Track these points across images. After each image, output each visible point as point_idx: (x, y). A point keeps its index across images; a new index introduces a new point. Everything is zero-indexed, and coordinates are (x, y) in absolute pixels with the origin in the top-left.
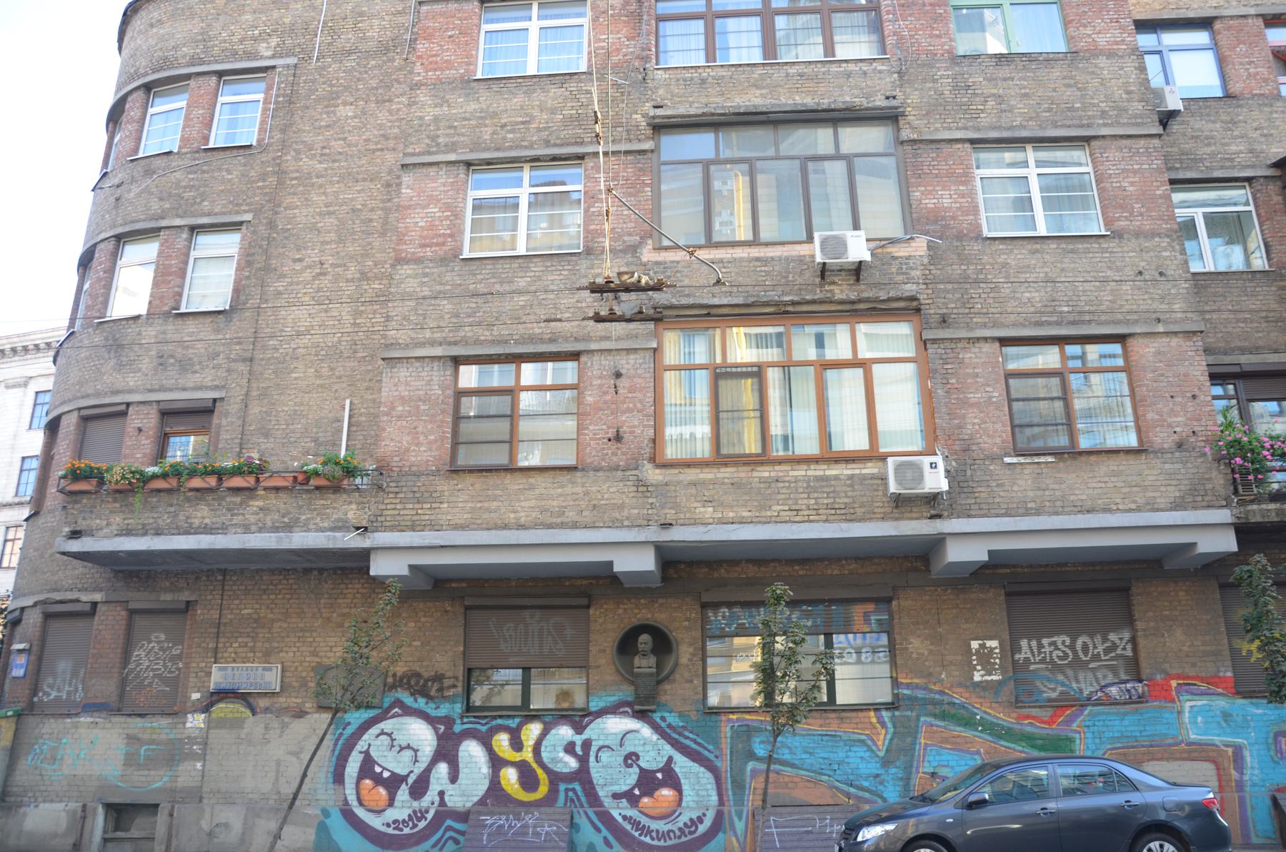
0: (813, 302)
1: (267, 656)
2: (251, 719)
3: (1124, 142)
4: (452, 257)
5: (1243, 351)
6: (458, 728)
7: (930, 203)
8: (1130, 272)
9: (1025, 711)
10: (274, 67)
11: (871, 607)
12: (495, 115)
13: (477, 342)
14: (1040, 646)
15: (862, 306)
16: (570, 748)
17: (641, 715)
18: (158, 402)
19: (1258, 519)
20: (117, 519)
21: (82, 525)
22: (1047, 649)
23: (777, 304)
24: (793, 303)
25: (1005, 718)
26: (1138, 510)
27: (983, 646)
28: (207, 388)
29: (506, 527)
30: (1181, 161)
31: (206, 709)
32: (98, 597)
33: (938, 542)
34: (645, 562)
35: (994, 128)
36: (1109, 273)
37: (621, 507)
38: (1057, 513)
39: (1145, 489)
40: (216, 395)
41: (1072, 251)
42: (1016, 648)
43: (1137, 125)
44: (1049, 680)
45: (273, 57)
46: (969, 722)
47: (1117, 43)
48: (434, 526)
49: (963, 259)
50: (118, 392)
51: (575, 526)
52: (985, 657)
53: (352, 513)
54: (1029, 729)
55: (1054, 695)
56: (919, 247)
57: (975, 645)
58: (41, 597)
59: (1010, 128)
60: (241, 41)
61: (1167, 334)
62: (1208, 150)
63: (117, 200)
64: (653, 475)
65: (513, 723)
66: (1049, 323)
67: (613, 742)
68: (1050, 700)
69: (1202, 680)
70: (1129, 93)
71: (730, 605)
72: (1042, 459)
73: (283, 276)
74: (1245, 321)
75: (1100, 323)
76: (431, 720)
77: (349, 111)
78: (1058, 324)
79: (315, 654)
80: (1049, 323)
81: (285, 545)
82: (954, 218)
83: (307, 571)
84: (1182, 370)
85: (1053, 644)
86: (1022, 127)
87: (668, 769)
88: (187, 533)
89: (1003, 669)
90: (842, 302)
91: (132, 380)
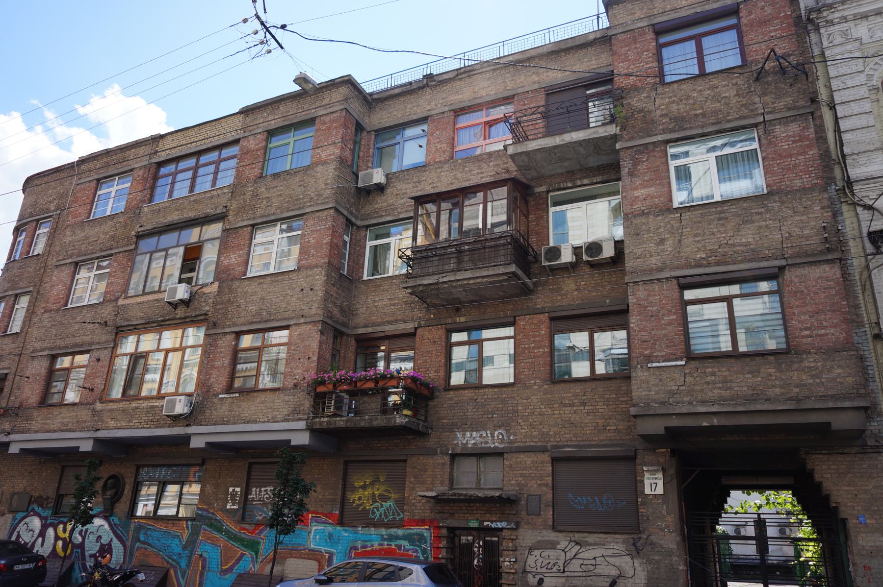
0: (169, 320)
3: (318, 214)
5: (389, 323)
6: (48, 522)
7: (226, 262)
8: (298, 290)
9: (244, 526)
11: (197, 468)
14: (260, 492)
15: (188, 320)
16: (80, 533)
17: (106, 518)
19: (318, 427)
22: (263, 494)
23: (157, 322)
24: (163, 321)
25: (234, 528)
26: (268, 421)
27: (234, 490)
30: (386, 211)
33: (187, 439)
35: (262, 217)
36: (289, 292)
37: (86, 421)
38: (234, 424)
39: (274, 411)
40: (6, 371)
41: (276, 281)
42: (247, 492)
43: (323, 203)
44: (260, 510)
46: (219, 530)
47: (330, 155)
48: (28, 431)
49: (231, 291)
51: (70, 430)
52: (234, 494)
54: (243, 535)
55: (260, 518)
56: (215, 287)
57: (231, 489)
59: (269, 215)
61: (305, 323)
62: (401, 201)
66: (256, 322)
67: (94, 530)
68: (258, 521)
69: (324, 515)
70: (326, 184)
71: (148, 466)
72: (234, 395)
74: (394, 305)
75: (277, 320)
76: (41, 518)
78: (259, 322)
80: (256, 322)
82: (233, 269)
84: (307, 343)
85: (266, 491)
86: (274, 214)
87: (110, 544)
89: (239, 503)
90: (180, 319)
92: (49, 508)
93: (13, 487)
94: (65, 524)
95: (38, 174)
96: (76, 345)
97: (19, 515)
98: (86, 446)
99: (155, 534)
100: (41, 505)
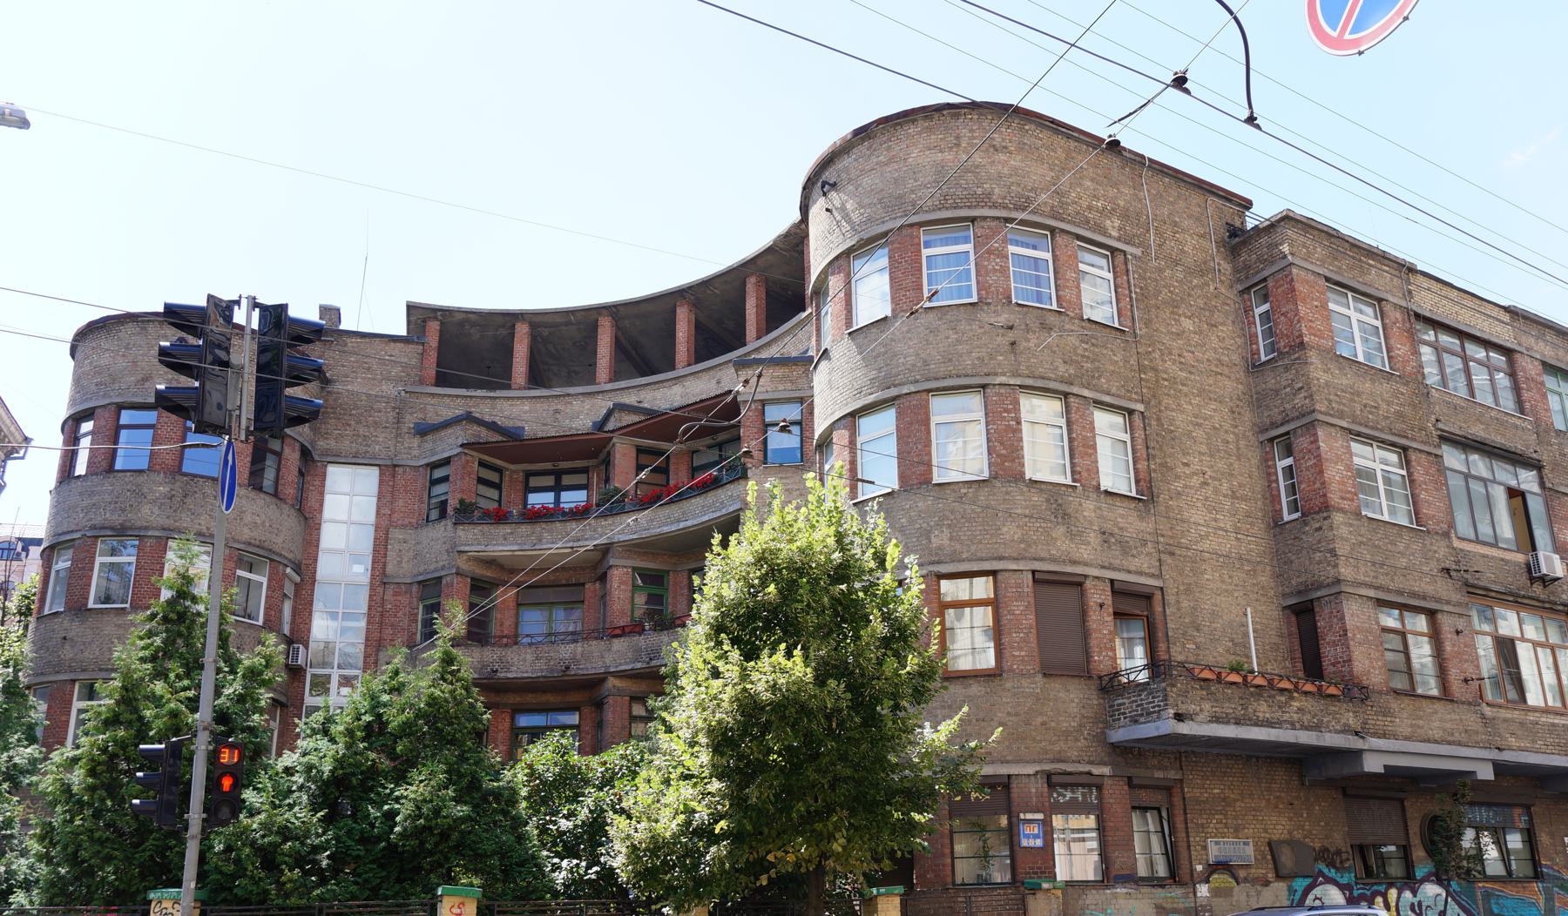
1: (1237, 831)
2: (1237, 888)
4: (1358, 514)
6: (1356, 893)
10: (1125, 252)
12: (1359, 394)
13: (1389, 591)
17: (1439, 882)
18: (1112, 581)
20: (1207, 706)
21: (1183, 709)
29: (1428, 741)
31: (1207, 881)
32: (1106, 770)
34: (1486, 773)
45: (1119, 239)
50: (1074, 563)
51: (1460, 744)
53: (1351, 719)
58: (1048, 767)
60: (1090, 208)
63: (1013, 344)
64: (1488, 711)
65: (1382, 888)
73: (1178, 477)
76: (1341, 887)
77: (1188, 324)
79: (1266, 831)
81: (1321, 743)
83: (1249, 758)
88: (1256, 725)
91: (1085, 553)
92: (1348, 870)
94: (1385, 896)
97: (1301, 884)
98: (1486, 773)
99: (1508, 903)
100: (1331, 864)
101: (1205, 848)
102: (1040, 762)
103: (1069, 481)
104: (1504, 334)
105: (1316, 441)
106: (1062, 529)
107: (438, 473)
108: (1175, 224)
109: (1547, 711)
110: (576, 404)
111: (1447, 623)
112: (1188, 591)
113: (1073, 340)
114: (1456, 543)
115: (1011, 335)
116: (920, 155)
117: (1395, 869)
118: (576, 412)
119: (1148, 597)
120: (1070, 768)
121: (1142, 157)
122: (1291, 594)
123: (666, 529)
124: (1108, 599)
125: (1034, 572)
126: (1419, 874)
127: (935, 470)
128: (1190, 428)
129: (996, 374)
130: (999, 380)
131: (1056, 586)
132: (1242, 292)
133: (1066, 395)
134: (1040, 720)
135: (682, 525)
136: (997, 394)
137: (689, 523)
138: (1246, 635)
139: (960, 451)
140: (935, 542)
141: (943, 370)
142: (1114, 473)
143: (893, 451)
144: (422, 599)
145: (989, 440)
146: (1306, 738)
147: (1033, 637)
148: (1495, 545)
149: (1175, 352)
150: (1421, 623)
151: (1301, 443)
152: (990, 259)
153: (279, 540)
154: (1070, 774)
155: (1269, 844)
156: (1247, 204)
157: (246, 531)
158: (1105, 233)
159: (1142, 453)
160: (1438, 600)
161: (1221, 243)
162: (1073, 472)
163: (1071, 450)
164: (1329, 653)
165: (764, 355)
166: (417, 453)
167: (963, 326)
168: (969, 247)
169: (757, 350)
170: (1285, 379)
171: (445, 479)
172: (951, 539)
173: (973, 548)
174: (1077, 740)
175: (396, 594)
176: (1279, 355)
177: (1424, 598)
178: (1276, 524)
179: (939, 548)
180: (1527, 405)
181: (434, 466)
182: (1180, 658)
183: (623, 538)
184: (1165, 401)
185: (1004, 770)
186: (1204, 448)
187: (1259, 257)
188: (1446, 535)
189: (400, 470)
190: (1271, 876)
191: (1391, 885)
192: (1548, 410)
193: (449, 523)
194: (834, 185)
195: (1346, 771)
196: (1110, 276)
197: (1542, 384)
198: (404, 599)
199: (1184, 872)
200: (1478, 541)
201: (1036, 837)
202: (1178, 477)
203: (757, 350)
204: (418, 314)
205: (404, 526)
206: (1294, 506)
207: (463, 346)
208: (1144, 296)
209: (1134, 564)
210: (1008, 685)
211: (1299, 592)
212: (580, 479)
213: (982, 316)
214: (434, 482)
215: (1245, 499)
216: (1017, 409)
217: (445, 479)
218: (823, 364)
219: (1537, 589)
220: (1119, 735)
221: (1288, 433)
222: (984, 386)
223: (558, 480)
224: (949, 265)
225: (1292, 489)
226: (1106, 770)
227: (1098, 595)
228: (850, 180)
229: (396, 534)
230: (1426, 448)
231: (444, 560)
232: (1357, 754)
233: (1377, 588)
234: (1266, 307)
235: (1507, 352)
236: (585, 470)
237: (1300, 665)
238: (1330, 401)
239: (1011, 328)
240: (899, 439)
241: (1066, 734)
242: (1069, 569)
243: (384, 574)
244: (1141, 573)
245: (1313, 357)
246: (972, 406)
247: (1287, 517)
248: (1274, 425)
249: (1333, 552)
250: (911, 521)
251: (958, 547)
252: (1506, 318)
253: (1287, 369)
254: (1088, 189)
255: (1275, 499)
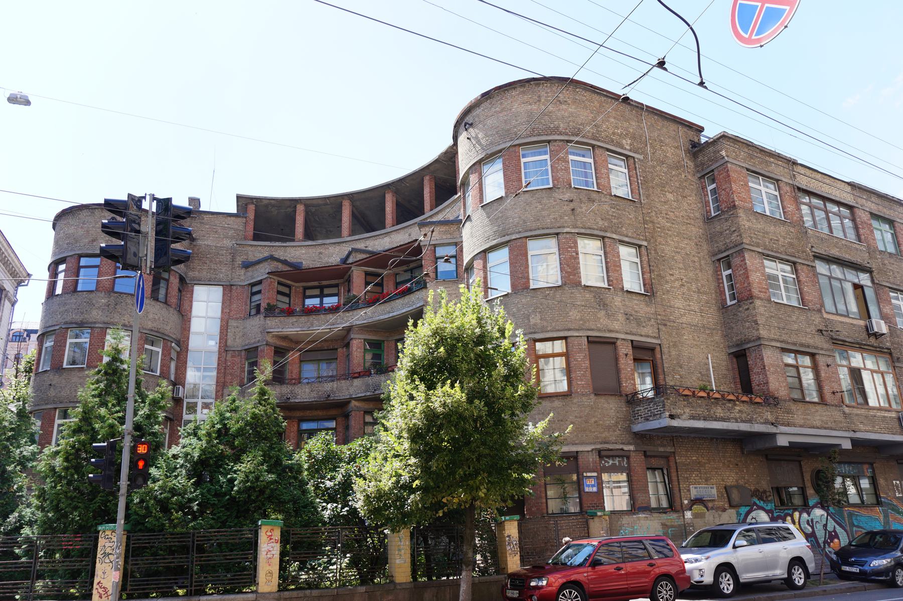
2: (707, 513)
4: (769, 300)
6: (775, 515)
10: (634, 158)
12: (767, 233)
13: (788, 343)
17: (823, 508)
18: (632, 341)
20: (687, 410)
21: (674, 412)
28: (651, 337)
31: (691, 509)
32: (632, 448)
34: (847, 445)
37: (841, 422)
45: (630, 151)
50: (610, 331)
51: (831, 429)
58: (599, 446)
60: (614, 134)
63: (573, 210)
64: (847, 410)
65: (790, 512)
73: (667, 282)
76: (767, 512)
77: (670, 196)
79: (723, 480)
83: (712, 439)
87: (835, 531)
88: (715, 420)
91: (616, 326)
92: (770, 501)
93: (723, 480)
95: (592, 86)
96: (802, 345)
97: (743, 510)
98: (847, 445)
99: (862, 519)
100: (760, 499)
101: (689, 491)
102: (594, 443)
103: (606, 286)
104: (849, 199)
105: (744, 260)
106: (603, 312)
107: (255, 289)
108: (661, 141)
109: (880, 409)
110: (331, 249)
111: (821, 361)
112: (675, 345)
113: (606, 207)
114: (825, 316)
115: (572, 205)
116: (519, 106)
117: (797, 501)
118: (329, 253)
119: (652, 350)
120: (611, 447)
121: (642, 104)
122: (733, 346)
123: (382, 317)
124: (630, 352)
125: (588, 337)
126: (811, 503)
127: (531, 281)
128: (673, 254)
129: (564, 227)
130: (566, 230)
131: (601, 345)
132: (700, 178)
133: (603, 238)
134: (593, 420)
135: (391, 315)
136: (565, 238)
137: (395, 314)
138: (708, 370)
139: (545, 269)
140: (532, 321)
141: (534, 225)
142: (631, 280)
143: (508, 271)
144: (247, 359)
145: (561, 264)
146: (744, 427)
147: (588, 374)
148: (847, 316)
149: (664, 212)
150: (807, 361)
151: (736, 261)
152: (559, 162)
153: (168, 328)
154: (612, 450)
155: (725, 488)
156: (700, 129)
157: (150, 323)
158: (622, 147)
159: (647, 269)
160: (816, 348)
161: (687, 151)
162: (608, 281)
163: (607, 268)
164: (755, 379)
165: (435, 219)
166: (244, 278)
167: (545, 201)
168: (547, 157)
169: (431, 217)
170: (725, 225)
171: (259, 292)
172: (541, 319)
173: (554, 324)
174: (615, 431)
175: (233, 356)
176: (722, 212)
177: (808, 347)
178: (723, 307)
179: (534, 325)
180: (863, 237)
181: (253, 285)
182: (672, 383)
183: (358, 323)
184: (659, 239)
185: (574, 449)
186: (681, 266)
187: (708, 159)
188: (819, 311)
189: (234, 288)
190: (727, 506)
191: (795, 510)
192: (874, 239)
193: (262, 316)
194: (471, 125)
195: (767, 445)
196: (626, 171)
197: (871, 225)
198: (237, 359)
199: (677, 504)
200: (837, 314)
201: (593, 486)
202: (667, 282)
203: (431, 217)
204: (243, 201)
205: (237, 319)
206: (733, 297)
207: (268, 218)
208: (645, 181)
209: (644, 331)
210: (575, 401)
211: (738, 345)
212: (334, 290)
213: (556, 195)
214: (253, 294)
215: (705, 293)
216: (576, 246)
217: (259, 292)
218: (468, 224)
219: (872, 340)
220: (638, 427)
221: (728, 256)
222: (557, 234)
223: (322, 292)
224: (536, 167)
225: (732, 287)
226: (632, 448)
227: (625, 349)
228: (480, 122)
229: (233, 323)
230: (806, 263)
231: (259, 337)
232: (773, 436)
233: (781, 342)
234: (714, 186)
235: (850, 208)
236: (337, 286)
237: (739, 386)
238: (751, 238)
239: (572, 201)
240: (511, 264)
241: (608, 428)
242: (608, 335)
243: (226, 345)
244: (648, 336)
245: (741, 213)
246: (550, 246)
247: (729, 303)
248: (721, 252)
249: (756, 322)
250: (519, 310)
251: (545, 324)
252: (849, 189)
253: (726, 220)
254: (612, 123)
255: (722, 293)
